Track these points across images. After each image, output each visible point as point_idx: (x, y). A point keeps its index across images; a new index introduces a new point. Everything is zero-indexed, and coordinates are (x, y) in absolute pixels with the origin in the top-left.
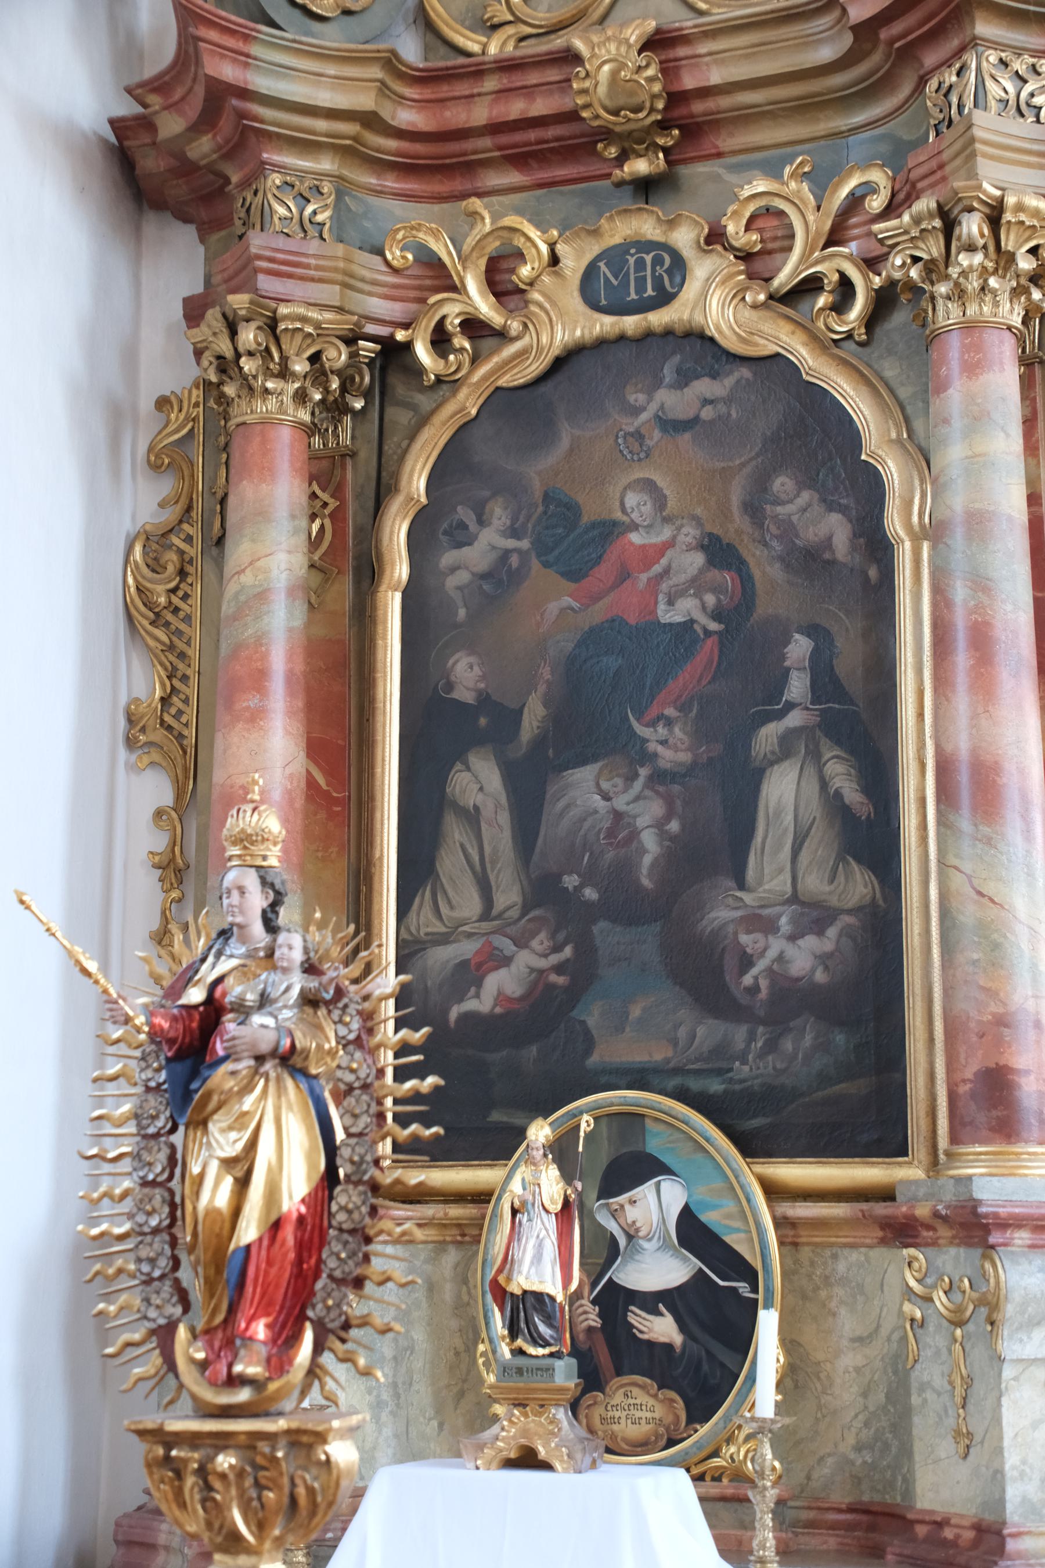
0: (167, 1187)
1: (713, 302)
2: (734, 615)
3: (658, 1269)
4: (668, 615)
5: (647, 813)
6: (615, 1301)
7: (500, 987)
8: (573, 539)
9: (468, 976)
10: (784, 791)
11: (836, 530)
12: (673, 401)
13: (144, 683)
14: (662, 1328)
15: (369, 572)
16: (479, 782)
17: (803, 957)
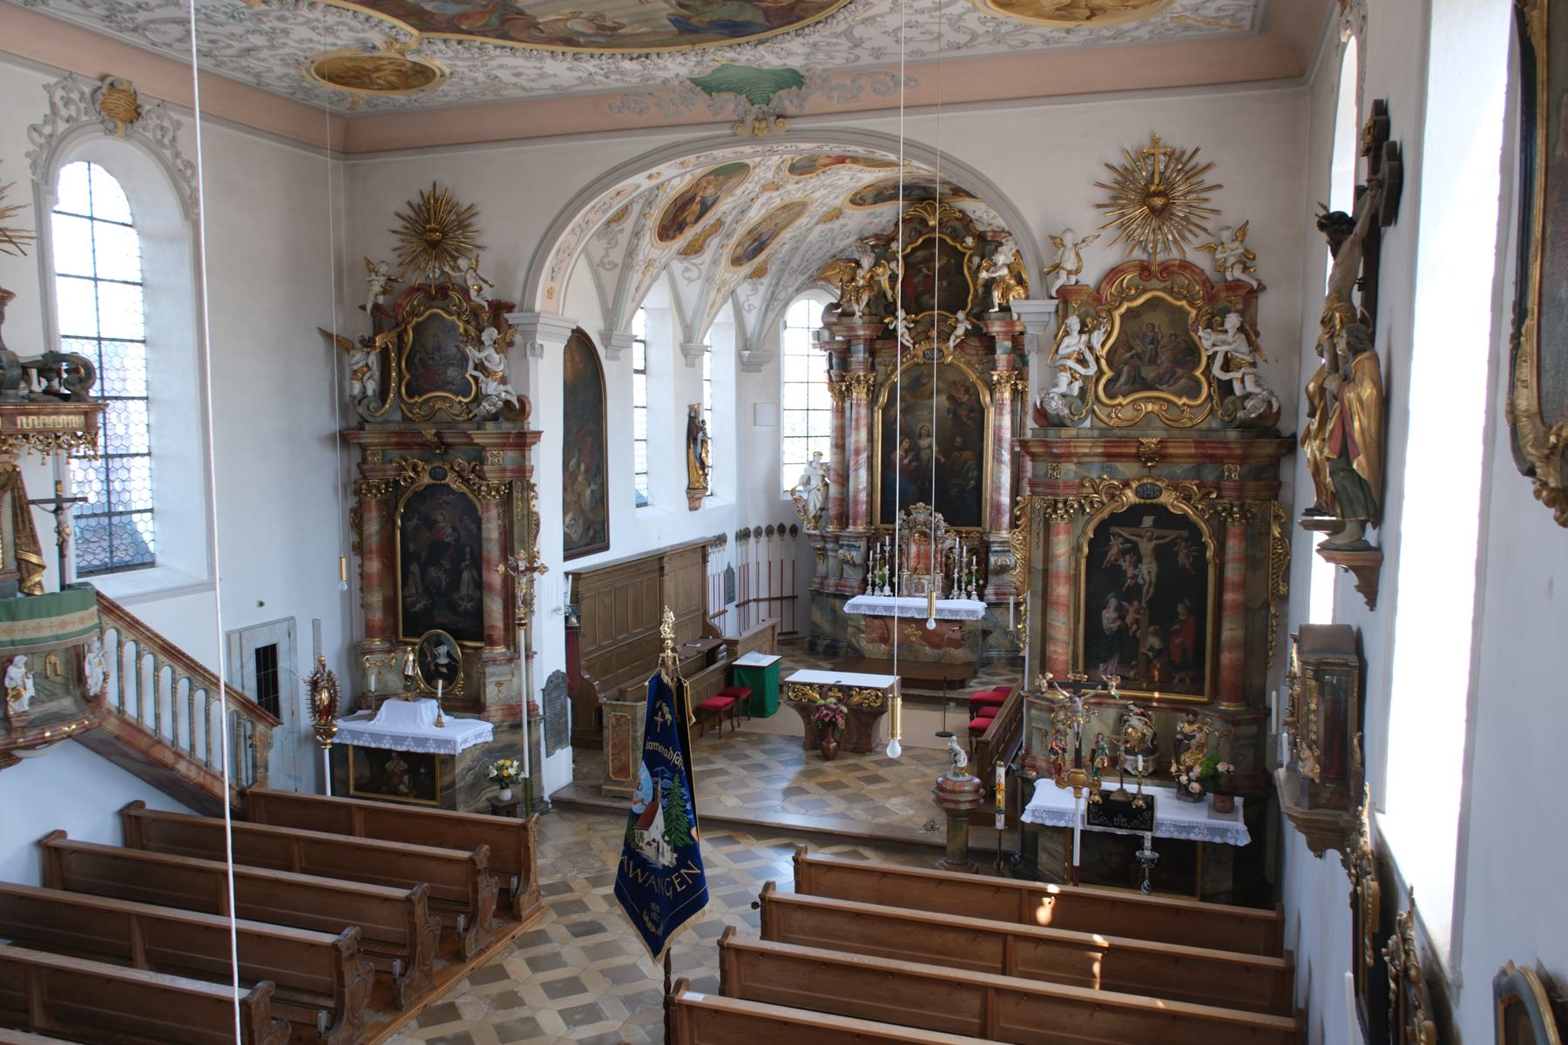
0: (313, 700)
1: (452, 480)
2: (457, 540)
3: (443, 661)
4: (447, 540)
5: (443, 577)
6: (437, 665)
7: (420, 606)
8: (430, 524)
9: (414, 604)
10: (466, 575)
11: (473, 526)
12: (447, 498)
13: (356, 539)
14: (444, 670)
15: (394, 523)
16: (415, 568)
17: (469, 606)
